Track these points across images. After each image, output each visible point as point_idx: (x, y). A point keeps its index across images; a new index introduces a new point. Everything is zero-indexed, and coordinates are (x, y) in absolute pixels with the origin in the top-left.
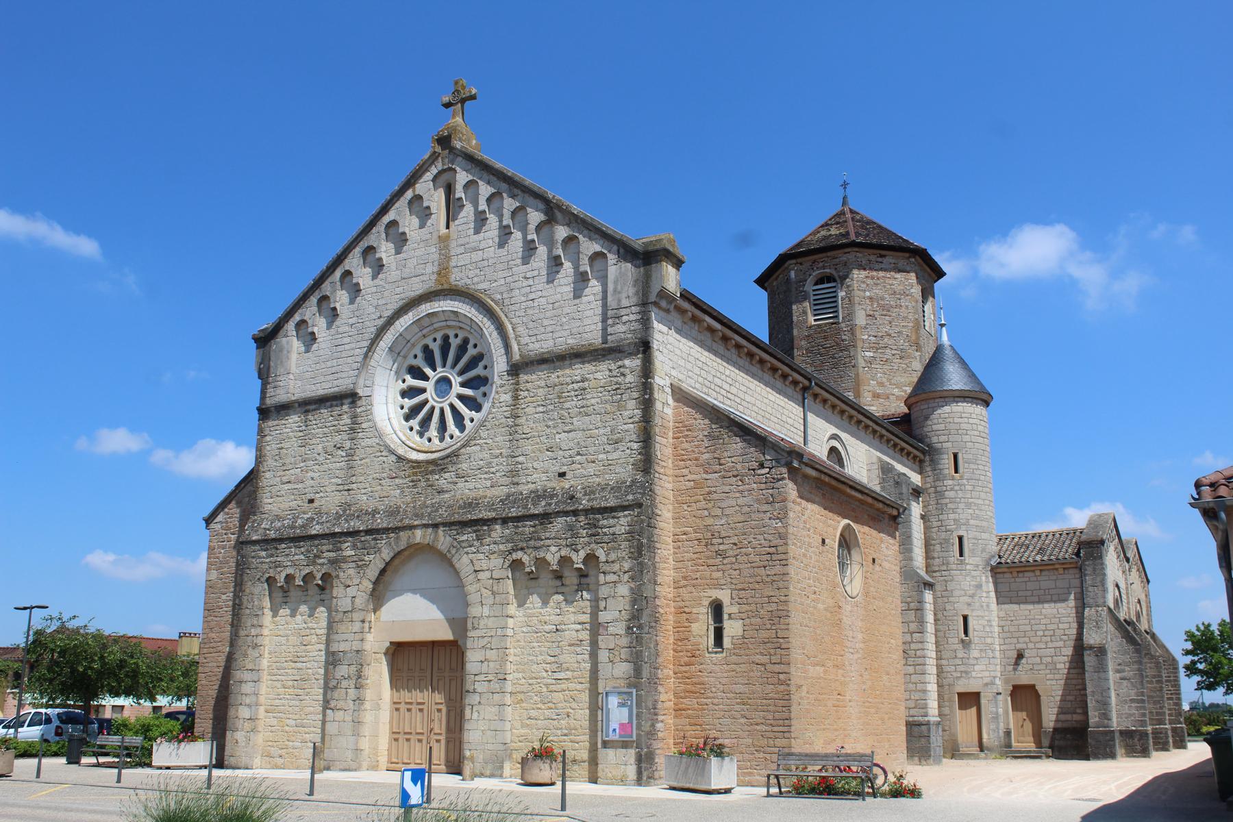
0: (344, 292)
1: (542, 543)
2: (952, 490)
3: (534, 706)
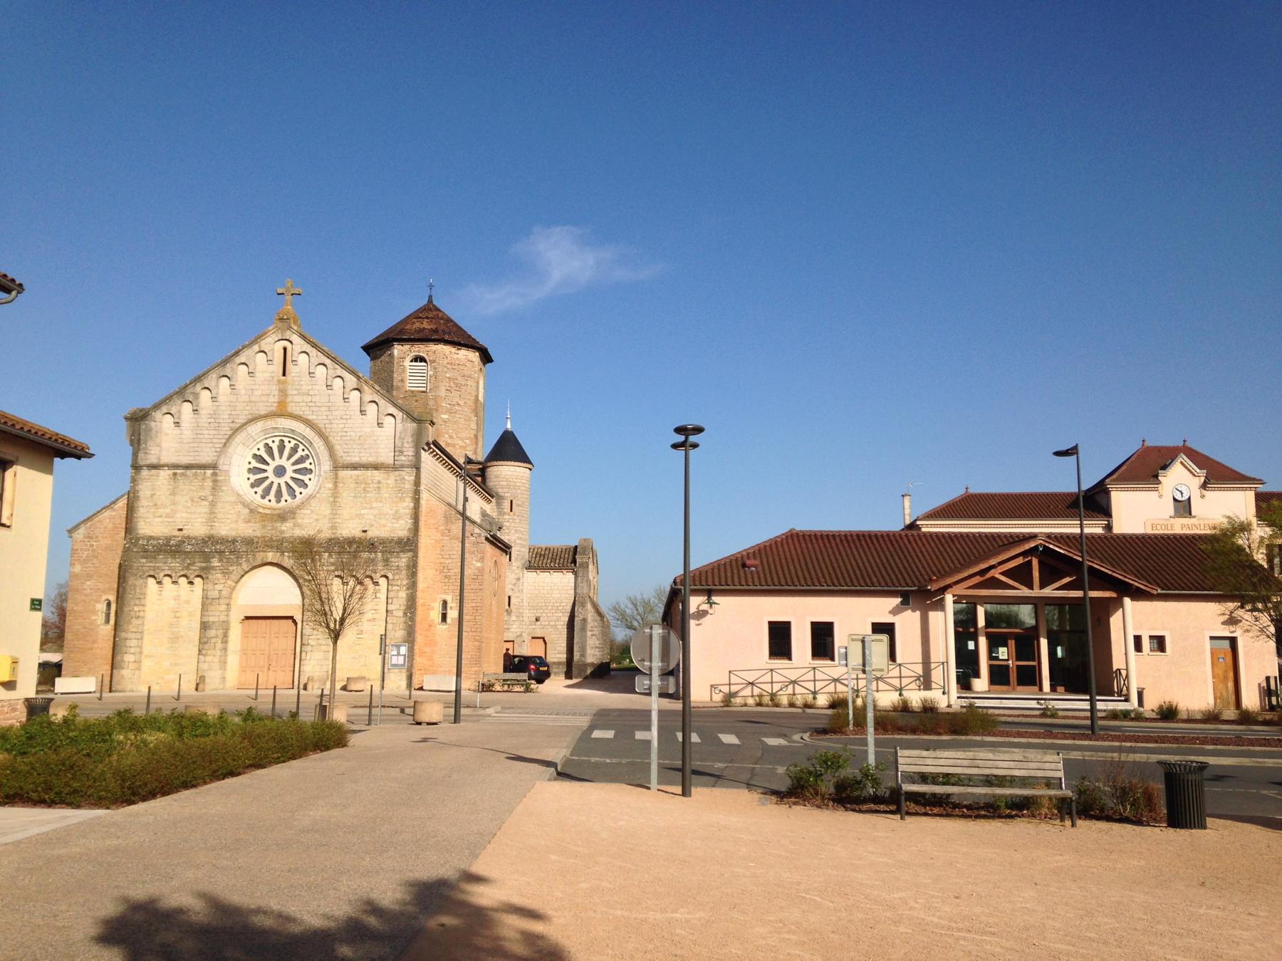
2: (508, 521)
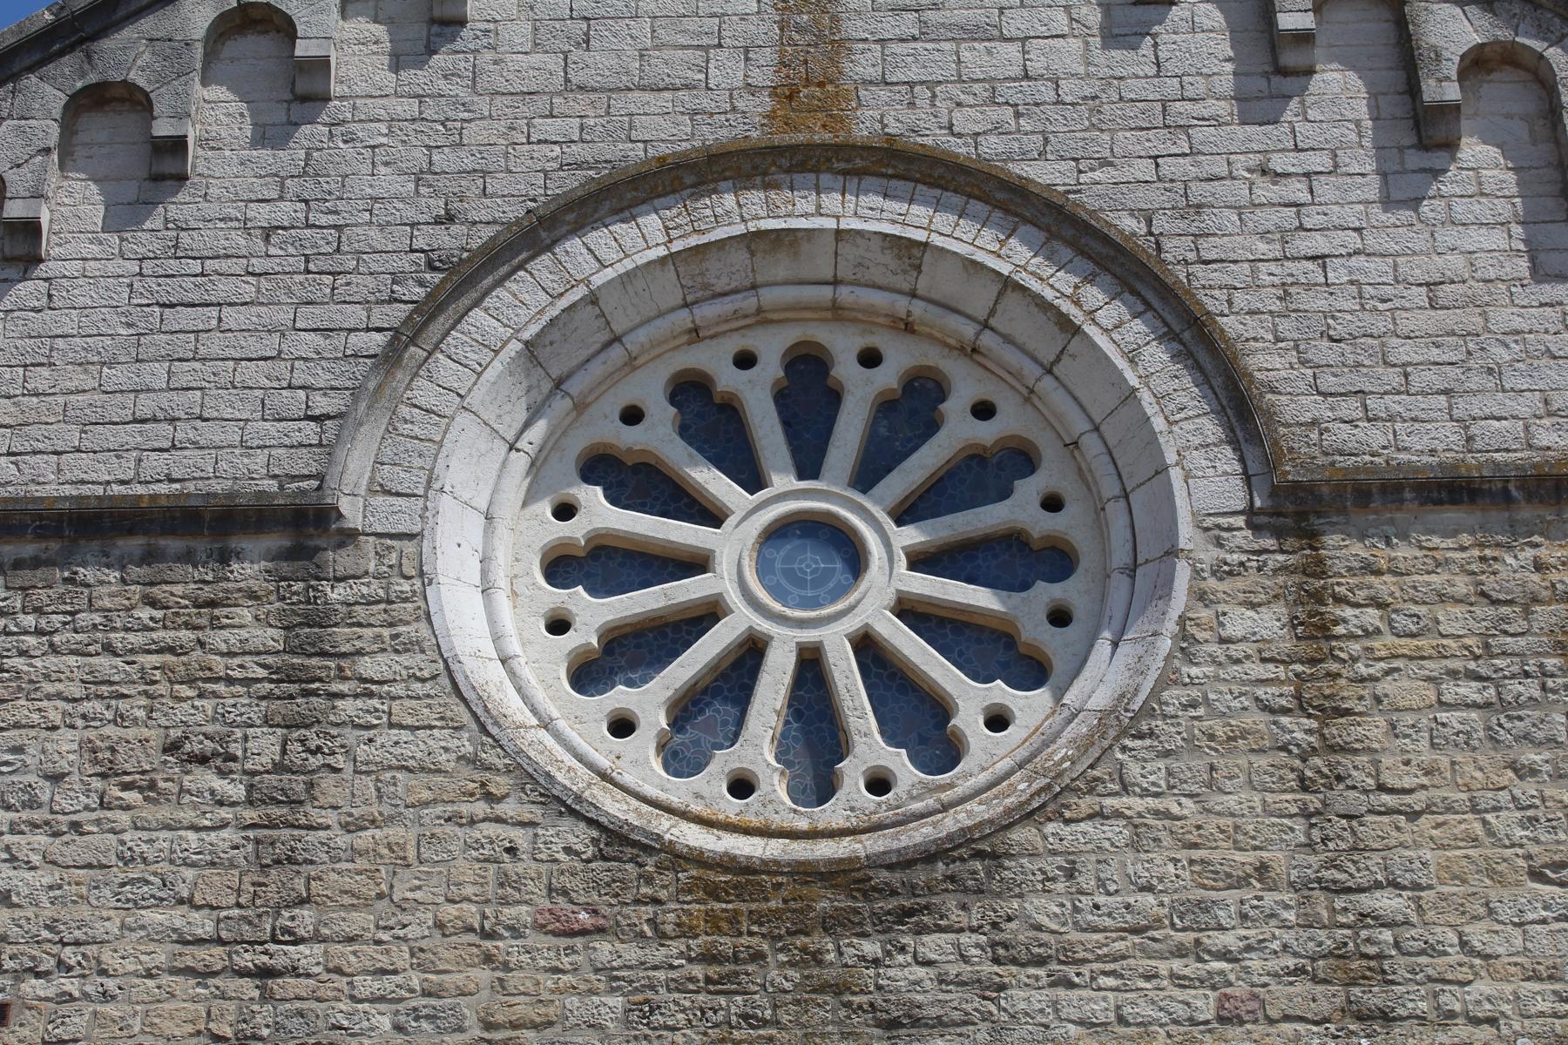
0: (218, 92)
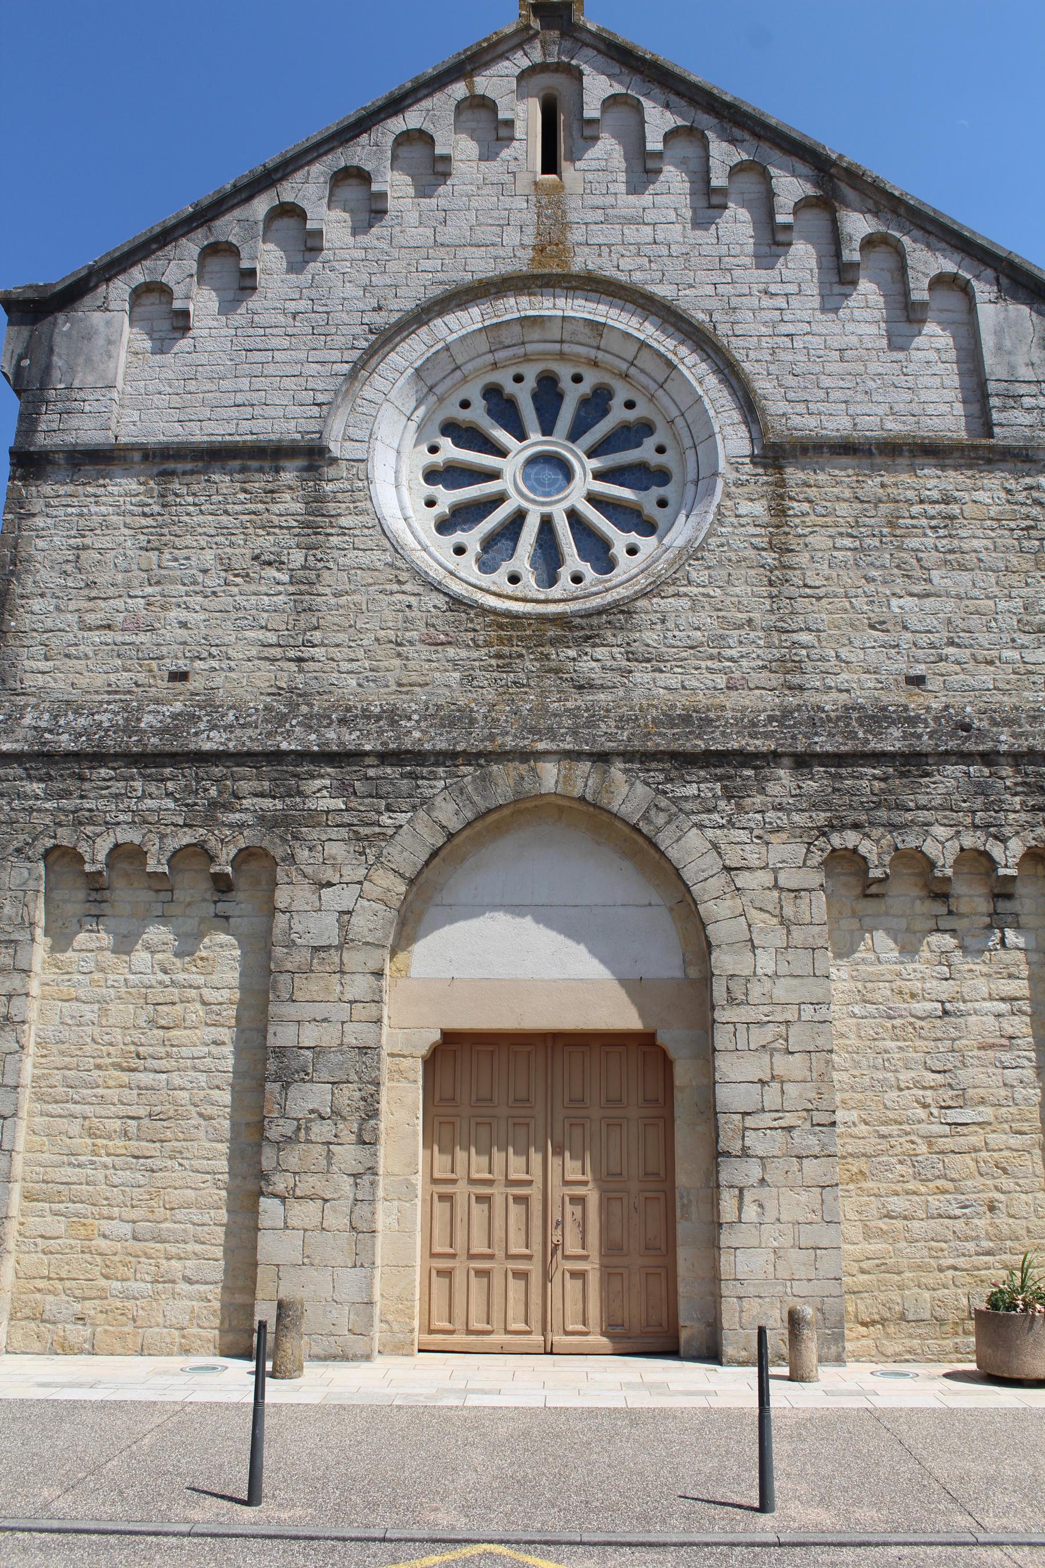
0: (270, 246)
1: (909, 816)
3: (898, 1187)
